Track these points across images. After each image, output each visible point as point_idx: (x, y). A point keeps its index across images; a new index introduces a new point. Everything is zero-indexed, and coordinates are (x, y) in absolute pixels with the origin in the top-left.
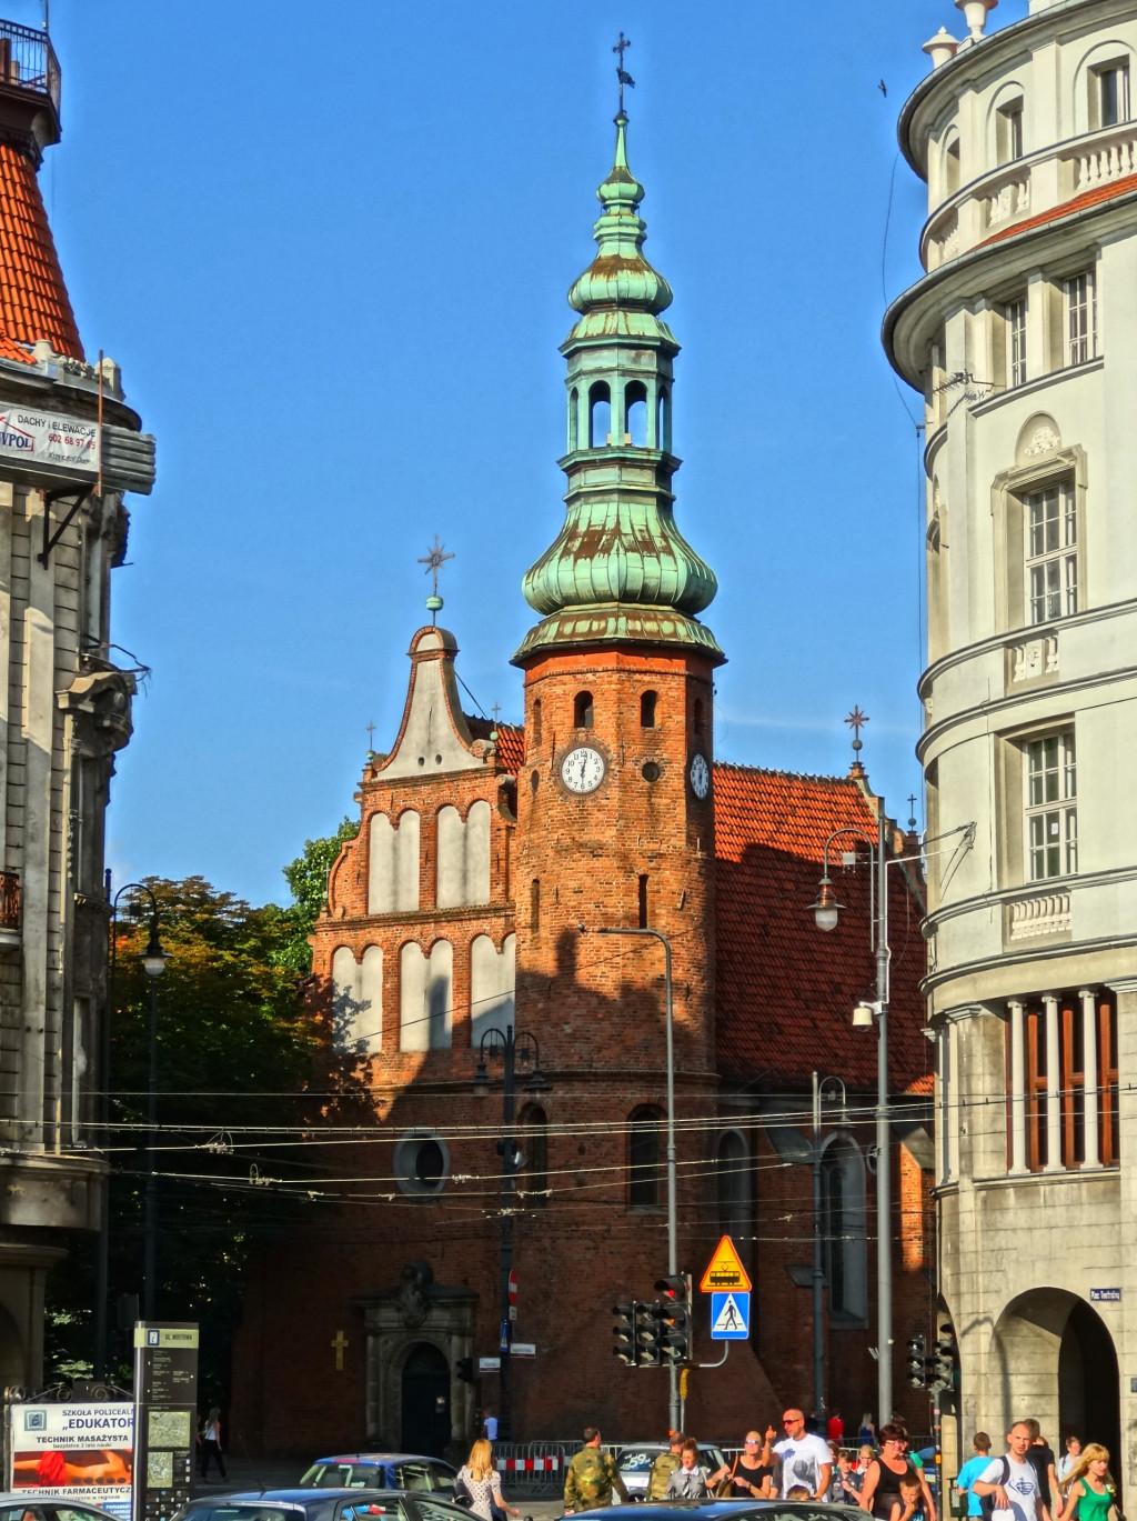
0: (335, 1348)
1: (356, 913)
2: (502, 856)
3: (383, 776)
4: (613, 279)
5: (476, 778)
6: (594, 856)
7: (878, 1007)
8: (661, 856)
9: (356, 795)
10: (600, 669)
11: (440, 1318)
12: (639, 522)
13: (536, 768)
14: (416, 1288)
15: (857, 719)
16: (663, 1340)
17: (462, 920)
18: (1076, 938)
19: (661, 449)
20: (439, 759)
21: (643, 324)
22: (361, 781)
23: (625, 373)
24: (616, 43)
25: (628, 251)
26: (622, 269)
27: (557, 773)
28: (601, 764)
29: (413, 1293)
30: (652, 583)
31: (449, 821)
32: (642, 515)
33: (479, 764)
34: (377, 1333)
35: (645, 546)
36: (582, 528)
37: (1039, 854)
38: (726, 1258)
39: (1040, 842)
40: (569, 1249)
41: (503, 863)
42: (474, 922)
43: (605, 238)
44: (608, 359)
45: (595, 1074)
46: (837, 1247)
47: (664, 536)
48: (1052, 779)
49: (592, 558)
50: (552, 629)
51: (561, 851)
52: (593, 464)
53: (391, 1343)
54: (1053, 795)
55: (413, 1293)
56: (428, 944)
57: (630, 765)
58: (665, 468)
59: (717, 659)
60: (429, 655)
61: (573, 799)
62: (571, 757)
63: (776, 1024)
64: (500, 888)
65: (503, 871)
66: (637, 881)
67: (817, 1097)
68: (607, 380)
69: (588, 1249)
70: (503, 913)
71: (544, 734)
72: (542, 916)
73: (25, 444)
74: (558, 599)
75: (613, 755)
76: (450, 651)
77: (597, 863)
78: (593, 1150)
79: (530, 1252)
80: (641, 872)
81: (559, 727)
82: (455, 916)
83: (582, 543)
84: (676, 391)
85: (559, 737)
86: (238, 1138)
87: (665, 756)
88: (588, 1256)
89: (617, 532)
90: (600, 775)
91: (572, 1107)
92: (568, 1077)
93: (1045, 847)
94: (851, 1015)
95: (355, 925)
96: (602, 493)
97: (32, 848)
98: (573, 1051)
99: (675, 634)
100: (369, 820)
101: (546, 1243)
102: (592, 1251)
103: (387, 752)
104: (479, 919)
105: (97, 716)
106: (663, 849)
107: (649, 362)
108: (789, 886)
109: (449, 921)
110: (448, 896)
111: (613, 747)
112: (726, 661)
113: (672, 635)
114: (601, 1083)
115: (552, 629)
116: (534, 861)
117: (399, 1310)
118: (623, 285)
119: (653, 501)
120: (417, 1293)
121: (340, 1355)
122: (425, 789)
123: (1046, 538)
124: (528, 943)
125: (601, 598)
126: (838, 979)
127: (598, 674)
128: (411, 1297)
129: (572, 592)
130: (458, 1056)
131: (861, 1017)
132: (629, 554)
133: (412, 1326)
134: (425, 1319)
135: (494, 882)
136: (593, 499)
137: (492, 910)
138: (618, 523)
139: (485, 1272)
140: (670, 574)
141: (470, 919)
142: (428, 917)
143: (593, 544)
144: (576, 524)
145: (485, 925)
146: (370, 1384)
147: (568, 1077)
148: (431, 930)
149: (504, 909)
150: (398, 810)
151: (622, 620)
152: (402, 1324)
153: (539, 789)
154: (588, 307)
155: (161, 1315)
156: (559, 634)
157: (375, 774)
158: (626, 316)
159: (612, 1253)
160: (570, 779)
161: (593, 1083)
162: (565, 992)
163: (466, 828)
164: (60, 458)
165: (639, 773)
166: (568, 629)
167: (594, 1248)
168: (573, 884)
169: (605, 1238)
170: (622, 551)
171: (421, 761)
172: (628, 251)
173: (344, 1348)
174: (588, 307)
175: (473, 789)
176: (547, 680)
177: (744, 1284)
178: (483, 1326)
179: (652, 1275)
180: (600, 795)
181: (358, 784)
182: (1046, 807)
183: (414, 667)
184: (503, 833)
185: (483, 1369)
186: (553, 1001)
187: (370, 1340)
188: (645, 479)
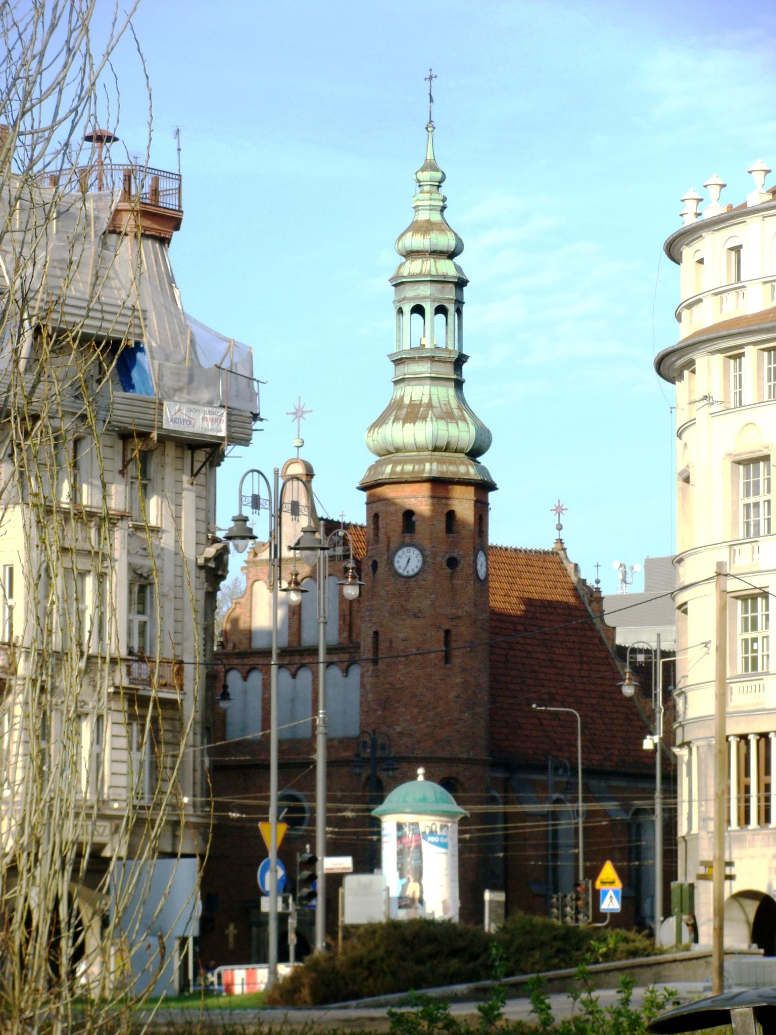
0: (228, 935)
1: (243, 647)
2: (347, 613)
4: (427, 237)
7: (656, 739)
8: (458, 617)
9: (243, 569)
12: (443, 399)
13: (376, 558)
15: (559, 510)
16: (577, 912)
18: (767, 707)
19: (456, 349)
21: (446, 267)
22: (246, 559)
24: (427, 75)
25: (436, 217)
26: (433, 230)
27: (390, 562)
28: (420, 558)
30: (453, 440)
32: (446, 393)
35: (448, 416)
36: (407, 401)
37: (746, 659)
38: (608, 871)
39: (746, 652)
44: (426, 290)
46: (555, 869)
47: (459, 408)
48: (755, 619)
49: (414, 423)
50: (389, 469)
52: (412, 359)
54: (755, 628)
56: (293, 669)
57: (439, 559)
58: (460, 361)
59: (492, 487)
62: (400, 553)
63: (517, 722)
64: (345, 634)
65: (347, 623)
66: (443, 634)
67: (658, 794)
68: (423, 304)
71: (382, 536)
73: (190, 423)
74: (392, 450)
75: (428, 553)
77: (417, 622)
80: (446, 627)
83: (407, 412)
84: (465, 309)
85: (393, 539)
86: (358, 811)
87: (461, 552)
89: (430, 405)
90: (420, 565)
93: (750, 655)
94: (642, 744)
95: (242, 655)
96: (418, 379)
97: (186, 644)
99: (468, 473)
100: (252, 586)
105: (216, 569)
106: (460, 612)
107: (450, 293)
108: (520, 627)
109: (309, 655)
111: (428, 547)
112: (497, 489)
113: (465, 474)
115: (389, 469)
116: (374, 620)
118: (434, 241)
119: (453, 384)
121: (231, 939)
123: (751, 489)
124: (370, 673)
125: (419, 449)
126: (553, 690)
131: (648, 744)
132: (439, 421)
136: (413, 383)
138: (430, 399)
140: (464, 435)
143: (413, 413)
144: (402, 398)
148: (297, 659)
149: (349, 648)
151: (435, 465)
154: (411, 254)
155: (494, 888)
156: (393, 472)
157: (256, 555)
158: (435, 262)
162: (397, 705)
164: (207, 430)
165: (444, 564)
166: (399, 469)
168: (402, 636)
170: (434, 419)
172: (436, 217)
174: (411, 254)
177: (618, 885)
180: (419, 577)
181: (246, 562)
182: (750, 635)
187: (254, 930)
188: (448, 371)
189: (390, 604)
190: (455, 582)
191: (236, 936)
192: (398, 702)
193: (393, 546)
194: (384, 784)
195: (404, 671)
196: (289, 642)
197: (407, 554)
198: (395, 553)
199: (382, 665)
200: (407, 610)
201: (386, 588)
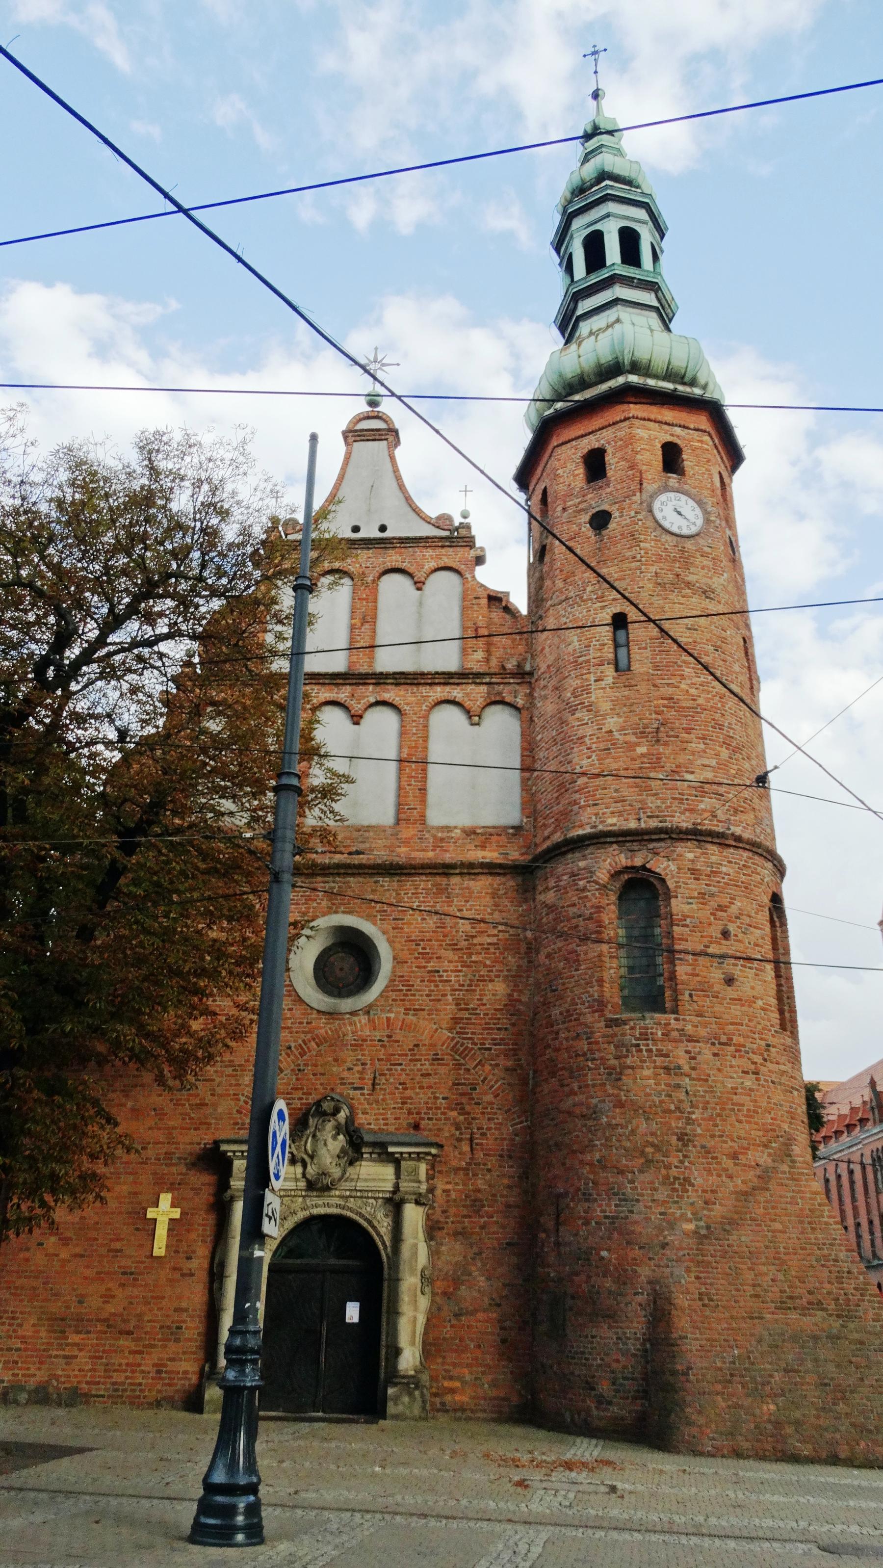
5: (443, 547)
6: (707, 597)
10: (692, 426)
11: (375, 1175)
14: (338, 1129)
17: (419, 684)
20: (383, 529)
29: (334, 1138)
33: (447, 533)
40: (719, 1070)
42: (439, 688)
43: (603, 149)
45: (738, 839)
55: (334, 1138)
61: (669, 538)
62: (663, 497)
64: (480, 655)
70: (487, 680)
78: (740, 936)
79: (646, 1072)
81: (644, 467)
85: (648, 476)
88: (748, 1083)
90: (700, 522)
91: (709, 876)
92: (697, 835)
98: (702, 806)
101: (683, 1060)
104: (445, 684)
109: (397, 684)
114: (741, 852)
120: (341, 1137)
121: (162, 1232)
124: (610, 680)
127: (687, 431)
128: (330, 1141)
130: (408, 832)
139: (454, 1114)
141: (431, 684)
145: (457, 693)
147: (697, 835)
148: (370, 693)
152: (302, 1184)
153: (612, 525)
159: (773, 1082)
160: (664, 518)
161: (732, 850)
163: (421, 596)
167: (754, 1073)
169: (765, 1060)
171: (356, 529)
175: (438, 557)
176: (627, 423)
180: (702, 542)
184: (485, 601)
186: (666, 744)
189: (653, 569)
192: (688, 731)
193: (649, 487)
194: (671, 884)
198: (653, 496)
200: (688, 584)
201: (642, 544)
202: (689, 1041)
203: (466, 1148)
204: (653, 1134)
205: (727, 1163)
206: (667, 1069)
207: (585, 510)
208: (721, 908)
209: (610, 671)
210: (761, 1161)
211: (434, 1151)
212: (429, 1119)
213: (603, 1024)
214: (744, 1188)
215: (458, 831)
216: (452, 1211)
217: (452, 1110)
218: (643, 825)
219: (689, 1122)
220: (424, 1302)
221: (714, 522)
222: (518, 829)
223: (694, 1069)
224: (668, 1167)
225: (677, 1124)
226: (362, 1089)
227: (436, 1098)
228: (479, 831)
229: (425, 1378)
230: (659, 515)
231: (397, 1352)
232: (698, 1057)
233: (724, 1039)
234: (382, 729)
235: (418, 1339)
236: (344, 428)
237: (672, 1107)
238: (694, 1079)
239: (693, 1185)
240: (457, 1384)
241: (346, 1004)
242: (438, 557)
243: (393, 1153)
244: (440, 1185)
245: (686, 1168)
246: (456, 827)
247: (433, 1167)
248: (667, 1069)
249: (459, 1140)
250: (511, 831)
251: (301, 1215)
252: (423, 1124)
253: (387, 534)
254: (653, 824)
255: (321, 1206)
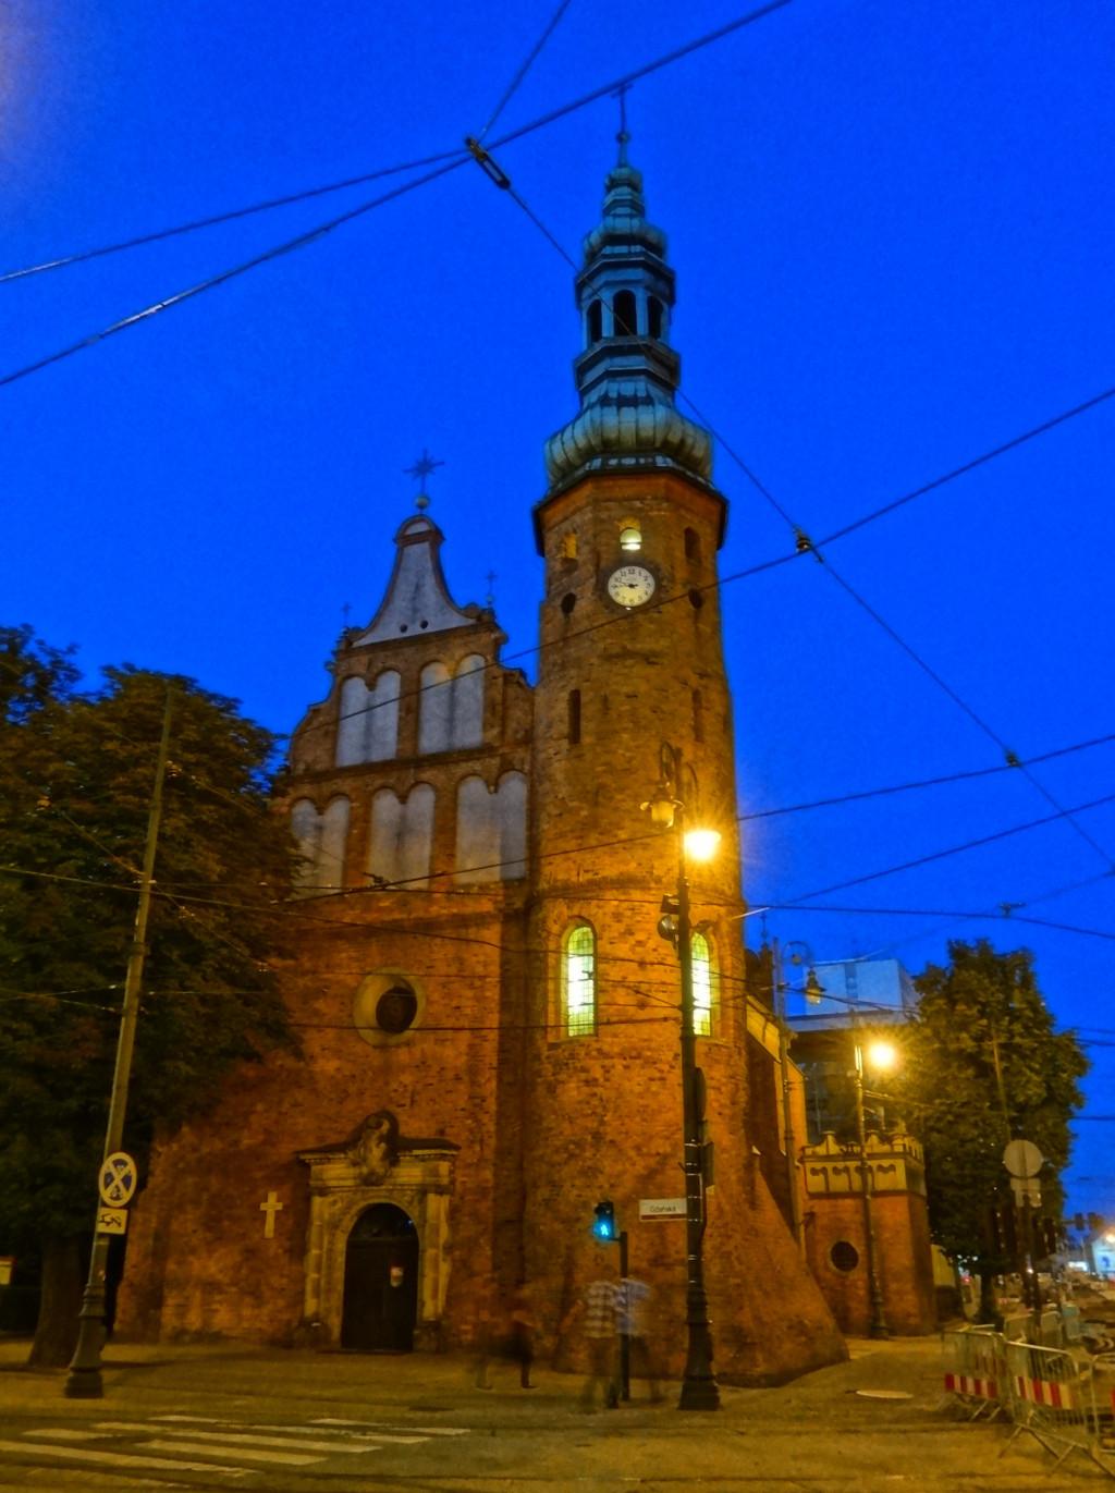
0: (265, 1212)
3: (356, 644)
9: (327, 664)
14: (381, 1139)
17: (447, 763)
20: (424, 625)
22: (335, 649)
23: (647, 288)
28: (651, 580)
29: (378, 1145)
31: (437, 674)
33: (471, 621)
34: (323, 1192)
40: (629, 1080)
41: (499, 708)
51: (608, 658)
53: (339, 1205)
60: (419, 538)
62: (617, 574)
64: (495, 731)
69: (652, 1079)
72: (583, 724)
76: (435, 537)
77: (651, 670)
79: (572, 1085)
81: (604, 548)
82: (440, 759)
88: (654, 1088)
90: (651, 590)
101: (598, 1073)
102: (658, 1083)
103: (363, 626)
110: (432, 740)
117: (355, 1164)
122: (408, 652)
129: (613, 436)
133: (369, 1181)
134: (391, 1176)
135: (486, 726)
137: (484, 750)
139: (469, 1122)
142: (406, 768)
145: (477, 766)
146: (314, 1252)
148: (410, 776)
150: (375, 671)
152: (358, 1181)
153: (576, 608)
160: (617, 594)
166: (613, 462)
168: (625, 689)
169: (672, 1067)
171: (404, 629)
173: (277, 1212)
178: (464, 1182)
179: (720, 1114)
183: (400, 551)
184: (500, 680)
185: (645, 1217)
187: (317, 1201)
190: (701, 626)
191: (277, 1212)
195: (632, 744)
196: (398, 751)
197: (629, 576)
199: (587, 740)
202: (605, 1058)
203: (477, 1148)
204: (574, 1135)
205: (632, 1153)
206: (587, 1082)
207: (559, 594)
208: (640, 943)
209: (565, 744)
210: (661, 1151)
211: (454, 1153)
212: (452, 1127)
213: (545, 1048)
214: (644, 1172)
215: (476, 888)
216: (467, 1198)
217: (468, 1118)
218: (581, 879)
219: (602, 1123)
220: (445, 1268)
221: (664, 587)
222: (521, 880)
223: (607, 1080)
224: (584, 1161)
225: (593, 1124)
226: (404, 1105)
227: (456, 1110)
228: (492, 886)
229: (444, 1323)
230: (612, 592)
231: (423, 1304)
232: (613, 1071)
233: (634, 1054)
234: (423, 802)
235: (442, 1296)
236: (394, 536)
237: (590, 1112)
238: (606, 1089)
239: (602, 1172)
240: (464, 1327)
241: (394, 1039)
242: (466, 644)
243: (416, 1156)
244: (460, 1179)
245: (598, 1160)
246: (474, 885)
247: (454, 1164)
248: (587, 1082)
249: (472, 1142)
250: (516, 884)
251: (362, 1204)
252: (448, 1130)
253: (429, 629)
254: (589, 876)
255: (378, 1196)
